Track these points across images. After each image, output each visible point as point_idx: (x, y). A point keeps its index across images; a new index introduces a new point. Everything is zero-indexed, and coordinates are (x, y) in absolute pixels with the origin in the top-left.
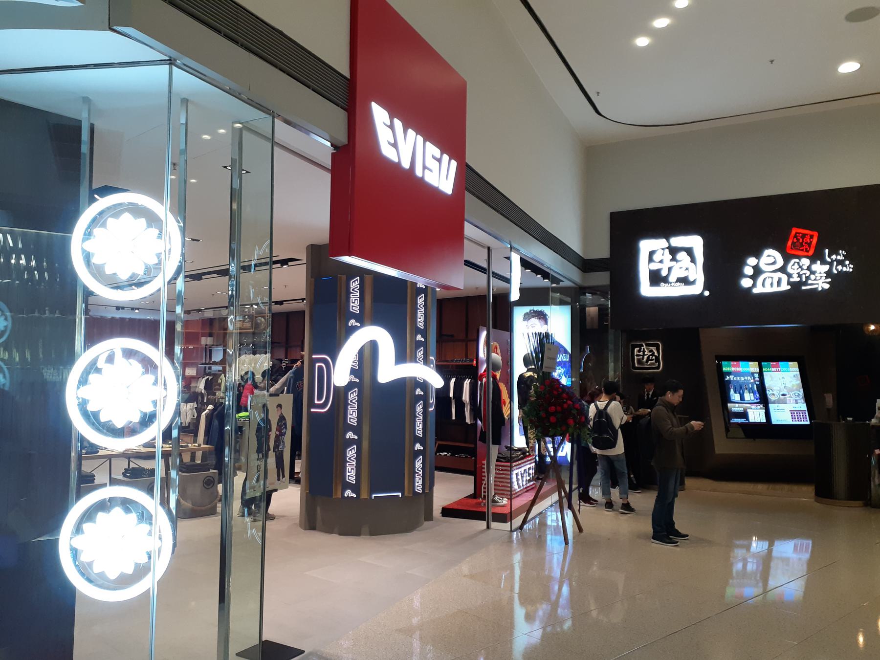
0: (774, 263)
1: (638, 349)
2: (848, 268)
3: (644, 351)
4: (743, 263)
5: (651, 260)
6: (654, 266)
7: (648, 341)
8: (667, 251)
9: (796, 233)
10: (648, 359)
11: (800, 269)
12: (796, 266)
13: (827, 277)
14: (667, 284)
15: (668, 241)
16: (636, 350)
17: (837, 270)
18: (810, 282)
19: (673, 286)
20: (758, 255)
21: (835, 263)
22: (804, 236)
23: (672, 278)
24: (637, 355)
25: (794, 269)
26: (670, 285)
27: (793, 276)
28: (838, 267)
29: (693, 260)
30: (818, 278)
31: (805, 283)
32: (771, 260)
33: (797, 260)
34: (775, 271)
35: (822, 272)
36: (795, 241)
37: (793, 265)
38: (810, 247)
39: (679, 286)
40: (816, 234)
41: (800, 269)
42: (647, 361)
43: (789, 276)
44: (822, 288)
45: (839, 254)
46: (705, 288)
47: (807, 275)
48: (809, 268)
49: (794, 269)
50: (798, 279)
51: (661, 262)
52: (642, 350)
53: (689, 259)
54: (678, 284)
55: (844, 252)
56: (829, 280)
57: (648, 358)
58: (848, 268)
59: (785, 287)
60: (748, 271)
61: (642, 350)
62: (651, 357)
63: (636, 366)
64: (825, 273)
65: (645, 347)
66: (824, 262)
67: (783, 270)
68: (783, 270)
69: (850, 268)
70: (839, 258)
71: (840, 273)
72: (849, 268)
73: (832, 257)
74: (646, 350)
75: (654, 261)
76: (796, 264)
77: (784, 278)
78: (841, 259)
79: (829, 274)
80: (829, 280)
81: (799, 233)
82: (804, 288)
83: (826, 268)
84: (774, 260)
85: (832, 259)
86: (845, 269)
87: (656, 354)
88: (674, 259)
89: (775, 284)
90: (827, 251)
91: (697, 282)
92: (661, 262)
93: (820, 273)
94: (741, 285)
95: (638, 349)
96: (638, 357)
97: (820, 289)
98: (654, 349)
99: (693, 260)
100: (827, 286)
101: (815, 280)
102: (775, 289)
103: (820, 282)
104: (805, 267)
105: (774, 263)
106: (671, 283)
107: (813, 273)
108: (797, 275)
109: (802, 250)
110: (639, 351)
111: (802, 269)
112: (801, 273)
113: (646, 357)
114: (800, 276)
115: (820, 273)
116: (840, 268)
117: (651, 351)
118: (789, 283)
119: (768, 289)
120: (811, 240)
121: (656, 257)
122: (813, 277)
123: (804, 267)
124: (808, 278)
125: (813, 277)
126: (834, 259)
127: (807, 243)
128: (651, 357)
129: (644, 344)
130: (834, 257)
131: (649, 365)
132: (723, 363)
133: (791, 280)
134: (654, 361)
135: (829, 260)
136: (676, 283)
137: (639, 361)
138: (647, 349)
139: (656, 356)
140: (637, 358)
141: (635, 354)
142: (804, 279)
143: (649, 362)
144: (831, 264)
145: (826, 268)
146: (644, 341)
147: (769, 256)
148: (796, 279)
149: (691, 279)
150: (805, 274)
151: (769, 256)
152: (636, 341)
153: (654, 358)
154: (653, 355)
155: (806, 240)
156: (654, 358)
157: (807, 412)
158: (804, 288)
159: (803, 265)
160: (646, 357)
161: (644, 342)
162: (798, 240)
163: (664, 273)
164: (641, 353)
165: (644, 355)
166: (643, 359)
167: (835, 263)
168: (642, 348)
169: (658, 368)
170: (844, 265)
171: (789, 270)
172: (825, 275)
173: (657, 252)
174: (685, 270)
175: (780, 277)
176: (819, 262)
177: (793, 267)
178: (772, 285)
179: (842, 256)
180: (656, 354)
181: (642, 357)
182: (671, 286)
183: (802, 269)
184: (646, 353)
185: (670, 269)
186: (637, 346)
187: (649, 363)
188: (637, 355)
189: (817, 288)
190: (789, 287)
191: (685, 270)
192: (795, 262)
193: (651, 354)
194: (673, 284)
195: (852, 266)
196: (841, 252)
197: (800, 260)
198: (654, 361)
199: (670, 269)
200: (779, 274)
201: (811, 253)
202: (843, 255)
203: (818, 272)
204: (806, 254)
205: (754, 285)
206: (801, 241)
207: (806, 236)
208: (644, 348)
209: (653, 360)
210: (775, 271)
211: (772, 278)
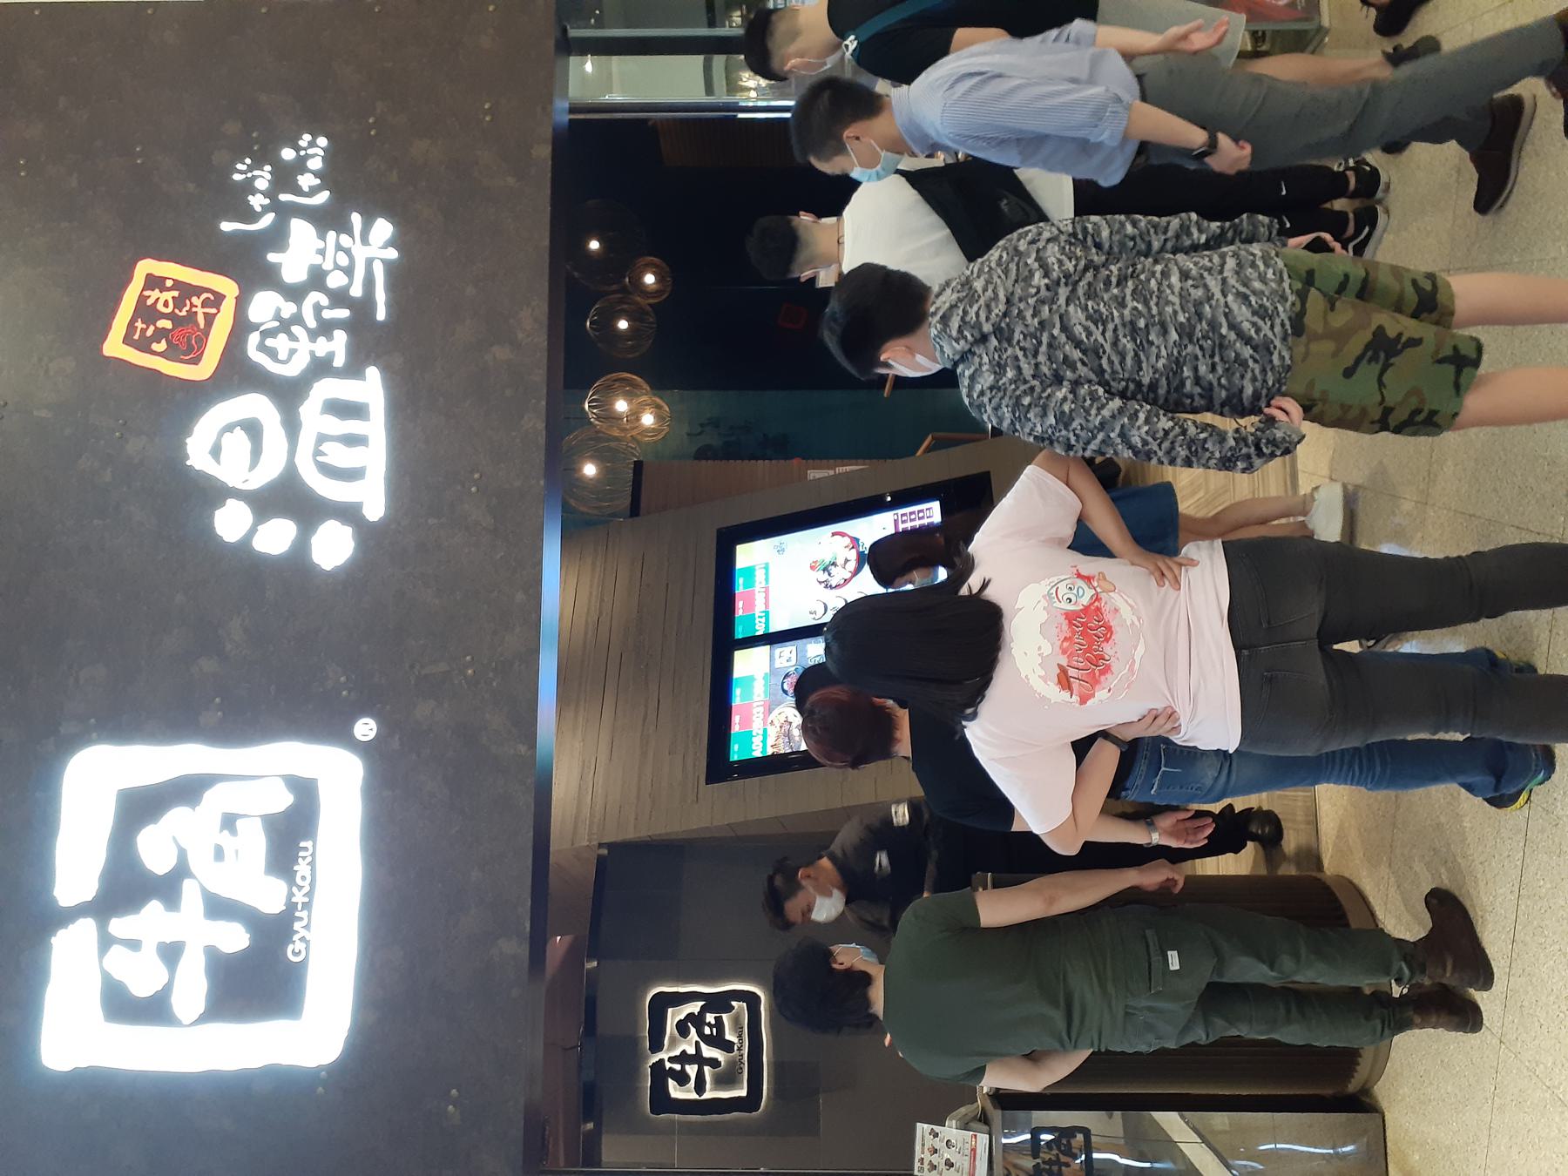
0: (253, 429)
1: (671, 1083)
2: (310, 151)
3: (683, 1058)
4: (243, 554)
5: (154, 1010)
6: (191, 991)
7: (634, 1041)
8: (119, 926)
9: (128, 340)
10: (718, 1041)
11: (296, 330)
12: (281, 343)
13: (344, 227)
14: (297, 926)
15: (67, 916)
16: (675, 1091)
17: (314, 191)
18: (356, 291)
19: (310, 894)
20: (213, 493)
21: (284, 197)
22: (145, 311)
23: (269, 897)
24: (700, 1087)
25: (293, 352)
26: (304, 914)
27: (321, 353)
28: (306, 189)
29: (187, 790)
30: (343, 260)
31: (363, 308)
32: (238, 443)
33: (254, 339)
34: (292, 426)
35: (321, 244)
36: (161, 347)
37: (272, 353)
38: (198, 290)
39: (312, 864)
40: (145, 267)
41: (296, 330)
42: (727, 1047)
43: (321, 368)
44: (385, 247)
45: (248, 187)
46: (340, 734)
47: (324, 300)
48: (295, 294)
49: (293, 352)
50: (341, 337)
51: (171, 953)
52: (678, 1067)
53: (176, 818)
54: (302, 868)
55: (240, 166)
56: (356, 219)
57: (709, 1041)
58: (310, 151)
59: (371, 388)
60: (276, 538)
61: (678, 1067)
62: (707, 1031)
63: (743, 1093)
64: (322, 237)
65: (664, 1055)
66: (277, 237)
67: (288, 394)
68: (288, 394)
69: (312, 144)
70: (262, 184)
71: (328, 178)
72: (315, 150)
73: (258, 209)
74: (677, 1052)
75: (167, 990)
76: (269, 342)
77: (326, 389)
78: (269, 177)
79: (328, 220)
80: (356, 219)
81: (131, 326)
82: (381, 315)
83: (300, 229)
84: (239, 433)
85: (266, 209)
86: (316, 164)
87: (695, 1007)
88: (167, 888)
89: (353, 426)
90: (227, 226)
91: (304, 772)
92: (171, 953)
93: (322, 252)
94: (338, 571)
95: (671, 1083)
96: (708, 1086)
97: (392, 254)
98: (674, 1016)
99: (187, 790)
100: (383, 229)
101: (349, 271)
102: (376, 427)
103: (361, 253)
104: (289, 309)
105: (253, 429)
106: (291, 907)
107: (317, 279)
108: (322, 340)
109: (210, 319)
110: (682, 1079)
111: (298, 319)
112: (312, 324)
113: (708, 1052)
114: (325, 329)
115: (322, 252)
116: (306, 181)
117: (682, 1028)
118: (354, 369)
119: (375, 457)
120: (169, 283)
121: (143, 979)
122: (335, 281)
123: (286, 315)
124: (339, 298)
125: (335, 281)
126: (267, 201)
127: (178, 302)
128: (707, 1031)
129: (655, 1058)
130: (257, 201)
131: (740, 1037)
132: (734, 757)
133: (339, 361)
134: (725, 1016)
135: (267, 220)
136: (298, 880)
137: (724, 1080)
138: (673, 1042)
139: (703, 1010)
140: (711, 1090)
141: (694, 1096)
142: (343, 313)
143: (729, 1036)
144: (285, 213)
145: (300, 229)
146: (636, 1058)
147: (216, 452)
148: (338, 346)
149: (282, 800)
150: (318, 309)
151: (216, 452)
152: (632, 1091)
153: (710, 1018)
154: (697, 1020)
155: (166, 304)
156: (710, 1018)
157: (901, 511)
158: (381, 315)
159: (277, 317)
160: (708, 1052)
161: (647, 1058)
162: (160, 334)
163: (234, 938)
164: (692, 1070)
165: (698, 1059)
166: (714, 1063)
167: (284, 197)
168: (668, 1065)
169: (751, 1000)
170: (300, 166)
171: (293, 369)
172: (332, 235)
173: (117, 976)
174: (233, 831)
175: (368, 473)
176: (272, 257)
177: (282, 356)
178: (352, 440)
179: (256, 173)
180: (695, 1007)
181: (707, 1069)
182: (307, 906)
183: (298, 319)
184: (691, 1051)
185: (218, 908)
186: (659, 1089)
187: (735, 1039)
188: (700, 1087)
189: (387, 264)
190: (373, 373)
191: (233, 831)
192: (262, 348)
193: (693, 1030)
194: (299, 898)
195: (307, 137)
196: (237, 177)
197: (256, 327)
198: (725, 1016)
199: (218, 908)
200: (310, 411)
201: (227, 287)
202: (250, 168)
203: (318, 260)
204: (228, 307)
205: (349, 514)
206: (167, 324)
207: (150, 302)
208: (671, 1060)
209: (719, 1021)
210: (292, 426)
211: (322, 438)
